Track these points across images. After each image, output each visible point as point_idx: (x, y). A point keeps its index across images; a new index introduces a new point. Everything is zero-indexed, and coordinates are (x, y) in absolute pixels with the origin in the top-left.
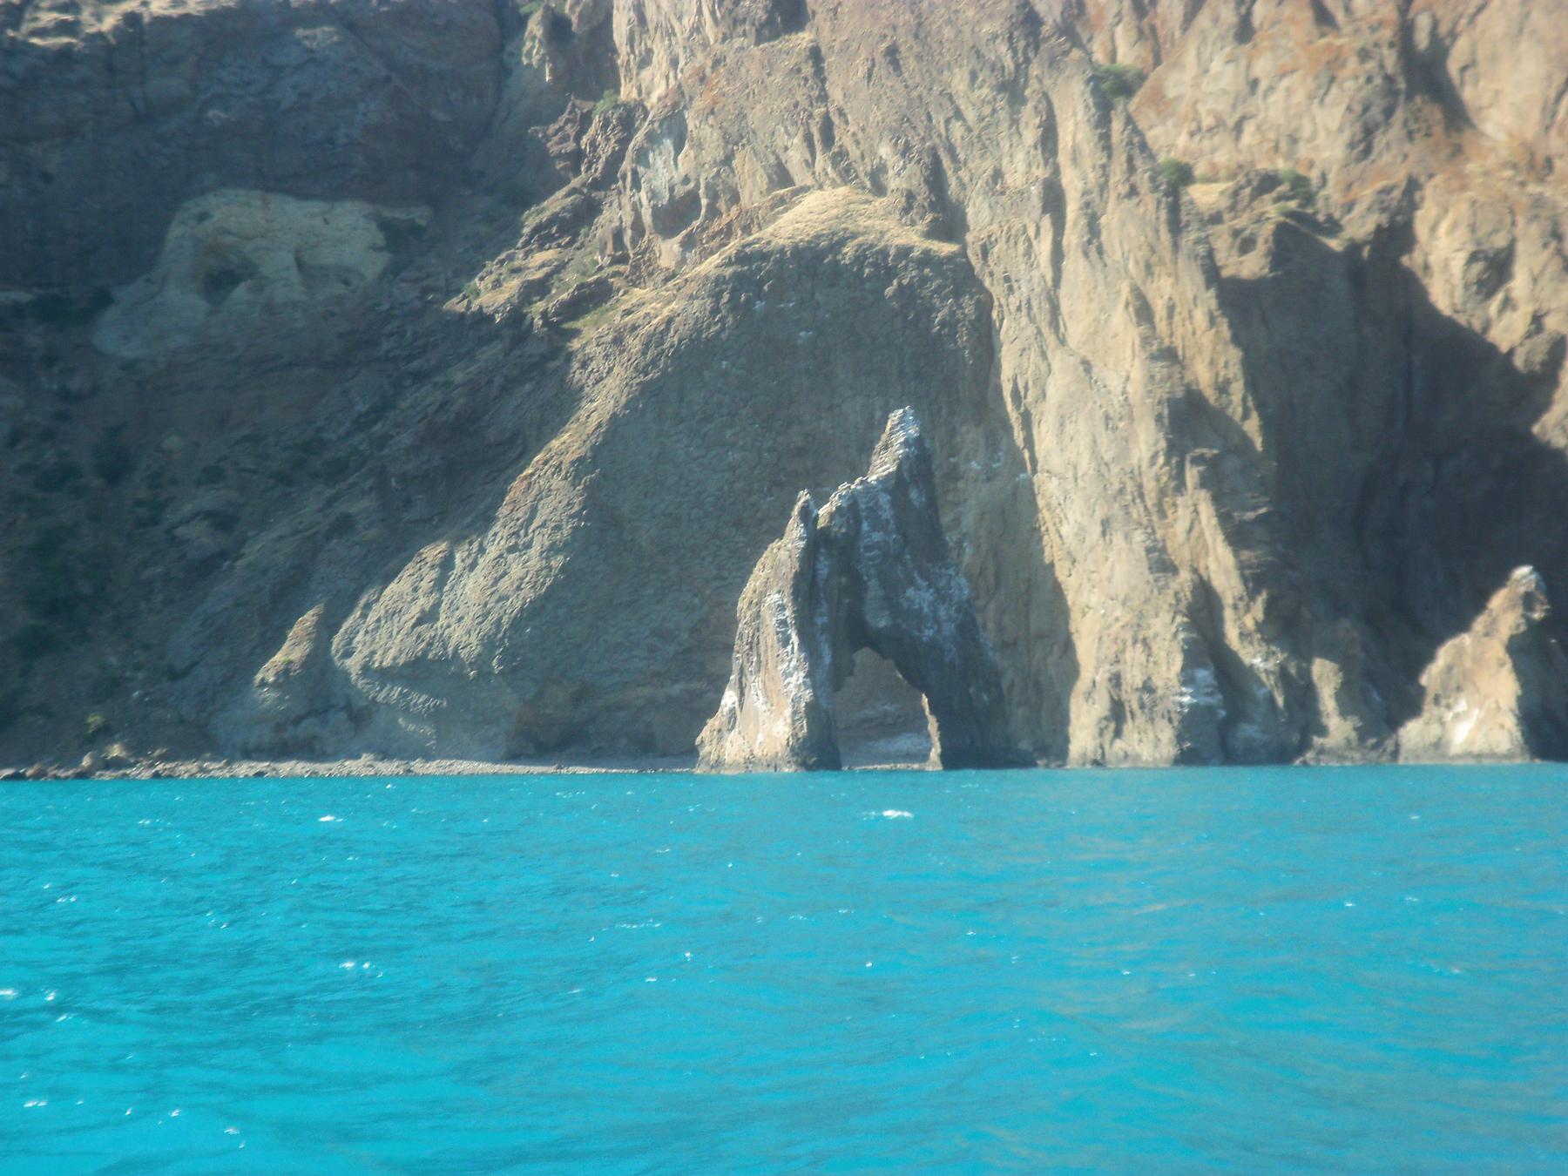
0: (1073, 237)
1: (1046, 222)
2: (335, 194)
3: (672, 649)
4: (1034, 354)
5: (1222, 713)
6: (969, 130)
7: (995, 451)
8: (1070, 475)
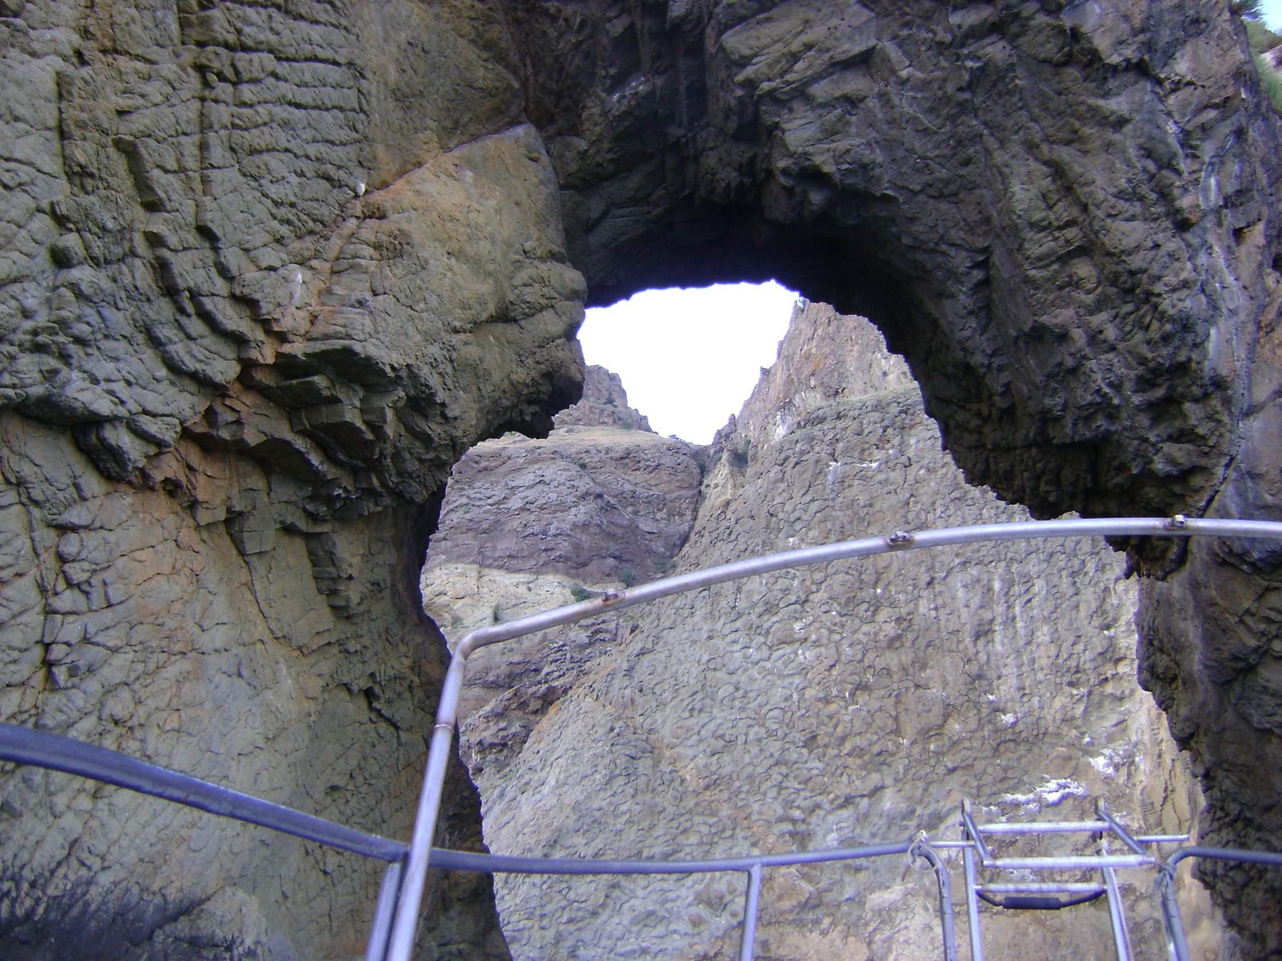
2: (539, 570)
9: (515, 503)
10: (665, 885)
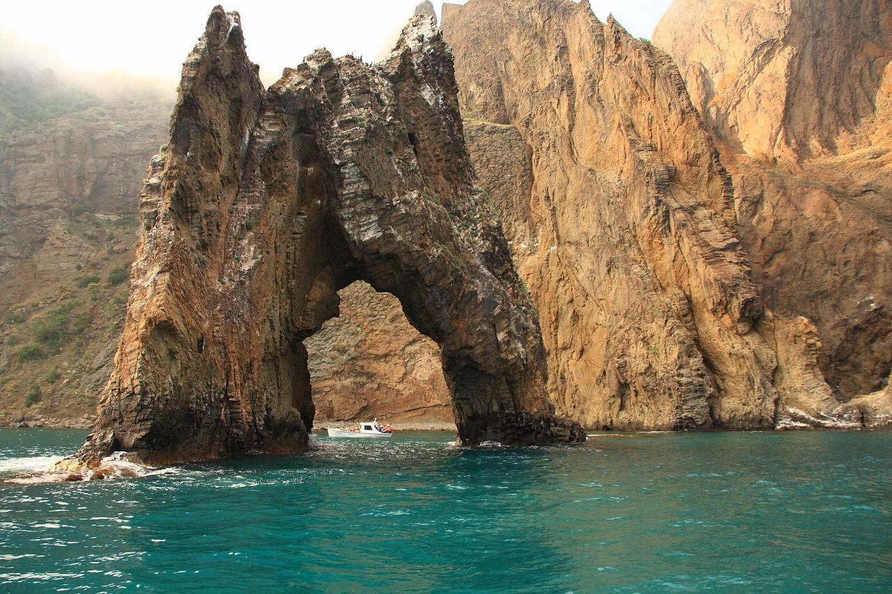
0: (580, 99)
1: (564, 96)
3: (345, 357)
4: (559, 174)
5: (711, 390)
6: (518, 64)
7: (536, 236)
8: (583, 241)
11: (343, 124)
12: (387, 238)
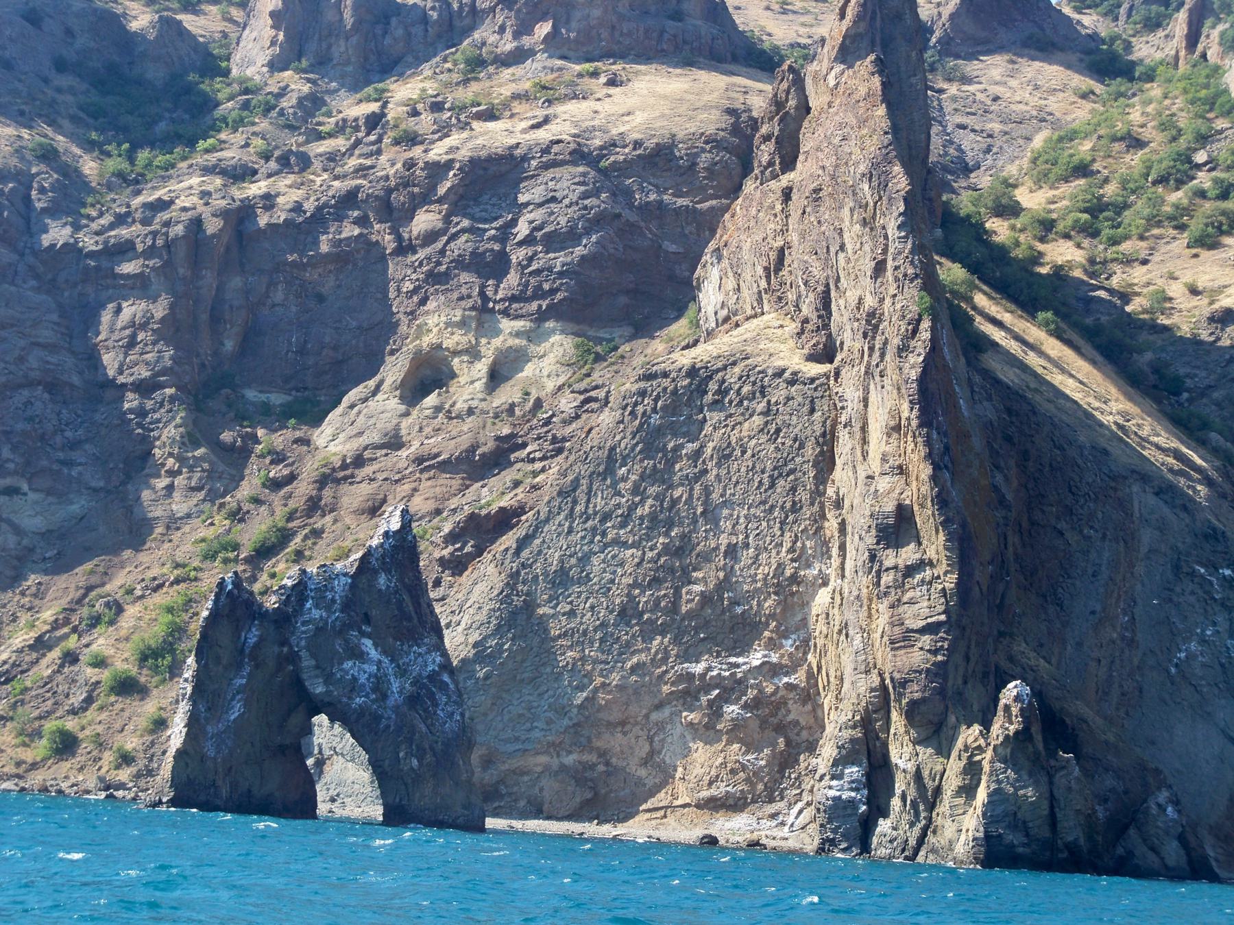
2: (541, 317)
9: (522, 229)
10: (531, 698)
11: (304, 623)
12: (328, 693)
